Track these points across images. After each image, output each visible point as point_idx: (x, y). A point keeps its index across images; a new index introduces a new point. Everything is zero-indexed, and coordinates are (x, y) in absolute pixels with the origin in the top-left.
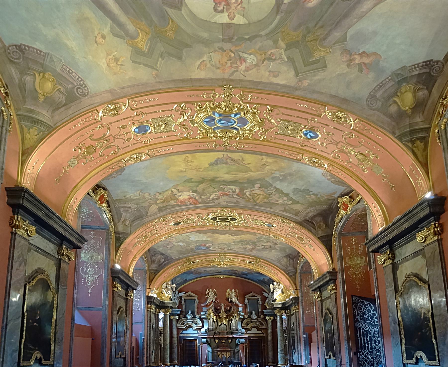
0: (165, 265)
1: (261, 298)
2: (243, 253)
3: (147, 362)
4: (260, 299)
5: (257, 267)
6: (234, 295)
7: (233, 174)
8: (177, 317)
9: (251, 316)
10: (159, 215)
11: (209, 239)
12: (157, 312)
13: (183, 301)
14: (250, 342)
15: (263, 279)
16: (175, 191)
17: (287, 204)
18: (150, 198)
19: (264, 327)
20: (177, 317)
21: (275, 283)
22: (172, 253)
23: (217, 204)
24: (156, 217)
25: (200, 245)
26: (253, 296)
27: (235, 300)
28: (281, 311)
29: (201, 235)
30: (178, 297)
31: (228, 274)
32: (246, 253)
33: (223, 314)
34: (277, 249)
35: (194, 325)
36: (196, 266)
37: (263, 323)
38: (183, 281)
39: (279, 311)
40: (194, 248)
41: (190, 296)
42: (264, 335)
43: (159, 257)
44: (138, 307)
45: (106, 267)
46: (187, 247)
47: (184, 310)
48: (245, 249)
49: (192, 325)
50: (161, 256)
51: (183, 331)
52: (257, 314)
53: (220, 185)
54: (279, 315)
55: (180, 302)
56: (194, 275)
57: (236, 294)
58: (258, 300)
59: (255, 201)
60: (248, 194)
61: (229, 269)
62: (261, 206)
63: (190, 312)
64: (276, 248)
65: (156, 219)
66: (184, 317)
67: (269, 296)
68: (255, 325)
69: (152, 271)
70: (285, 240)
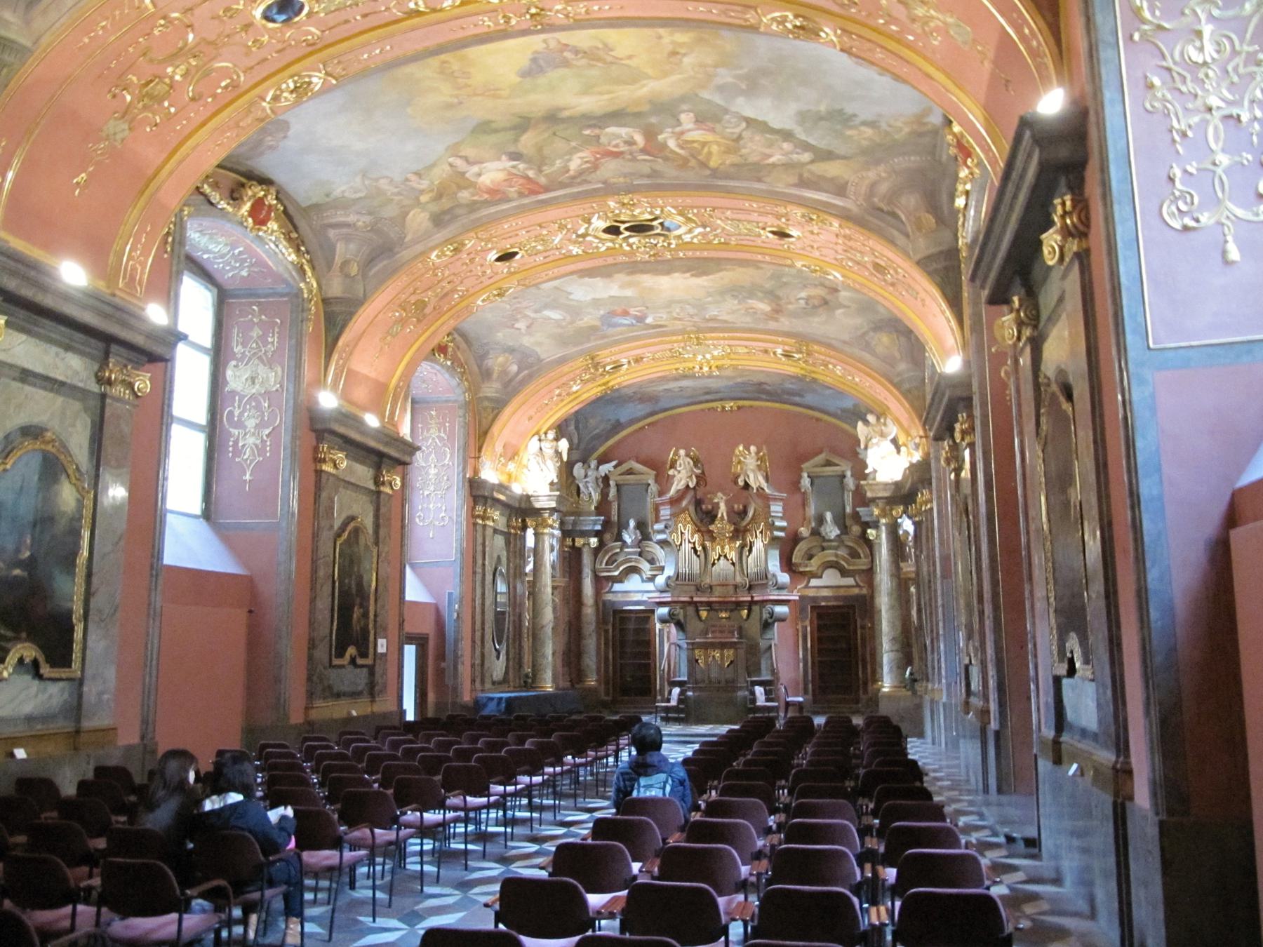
0: (524, 382)
2: (752, 325)
3: (473, 681)
4: (849, 473)
5: (809, 368)
6: (751, 462)
7: (601, 93)
8: (594, 541)
9: (822, 529)
10: (440, 236)
11: (628, 293)
12: (514, 528)
13: (613, 492)
14: (820, 616)
16: (459, 163)
17: (803, 165)
18: (396, 190)
19: (862, 564)
20: (594, 541)
21: (871, 418)
22: (540, 344)
23: (600, 185)
24: (431, 244)
25: (613, 314)
26: (828, 463)
27: (757, 480)
28: (891, 510)
29: (598, 282)
30: (597, 479)
31: (744, 395)
32: (761, 326)
33: (722, 525)
34: (849, 307)
35: (645, 566)
36: (626, 377)
38: (609, 427)
39: (883, 510)
40: (598, 323)
41: (630, 472)
42: (864, 591)
43: (501, 359)
44: (443, 514)
45: (291, 402)
46: (572, 322)
47: (615, 518)
48: (752, 312)
49: (640, 566)
50: (507, 355)
51: (613, 582)
52: (841, 521)
53: (581, 129)
54: (885, 525)
55: (604, 495)
56: (640, 407)
57: (759, 459)
58: (844, 476)
59: (704, 165)
60: (672, 144)
61: (739, 380)
62: (728, 177)
63: (632, 523)
64: (846, 303)
65: (432, 249)
66: (615, 541)
68: (834, 559)
69: (486, 404)
70: (843, 276)
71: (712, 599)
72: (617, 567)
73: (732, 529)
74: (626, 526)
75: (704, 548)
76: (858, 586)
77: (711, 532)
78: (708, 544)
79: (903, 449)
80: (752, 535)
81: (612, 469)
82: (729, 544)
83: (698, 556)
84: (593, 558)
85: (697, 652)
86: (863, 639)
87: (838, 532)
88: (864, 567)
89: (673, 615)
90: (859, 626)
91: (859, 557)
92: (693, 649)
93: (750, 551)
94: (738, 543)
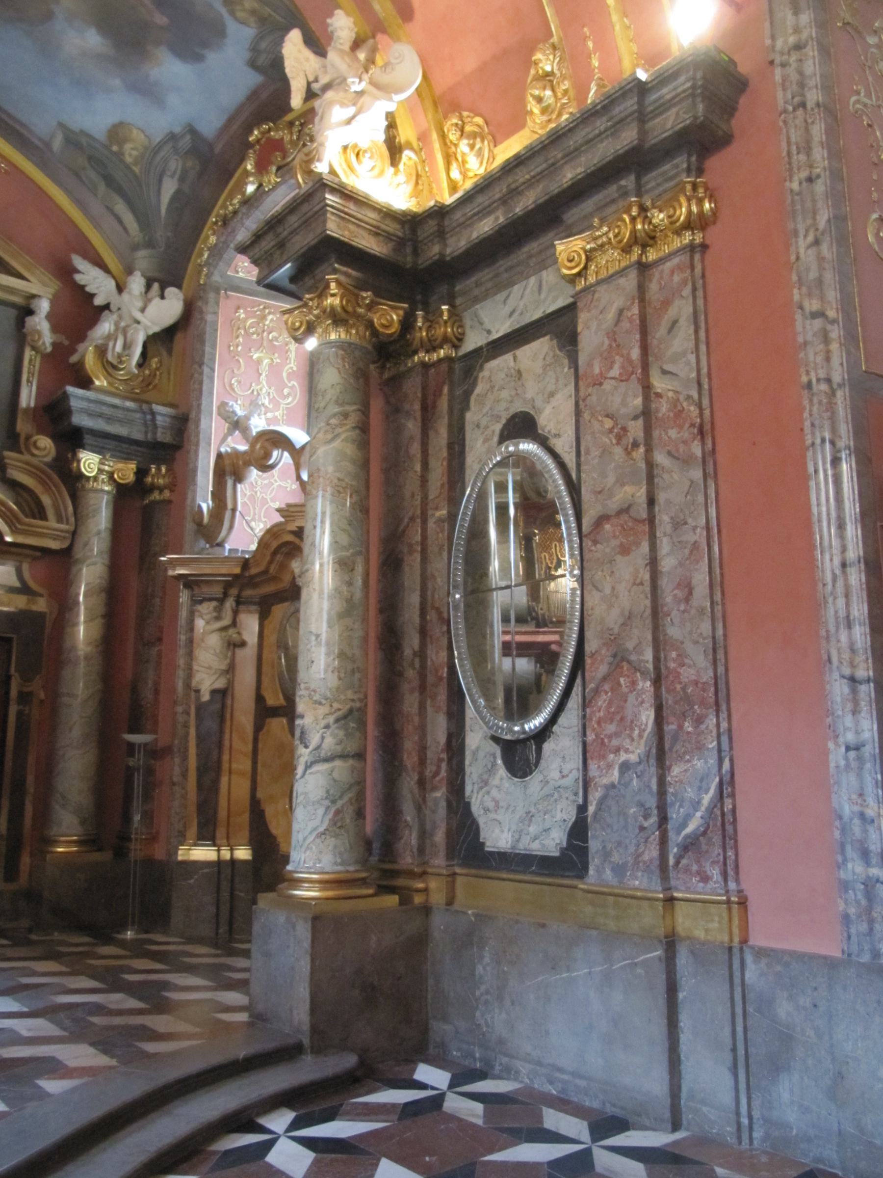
1: (53, 302)
4: (44, 306)
15: (117, 132)
37: (46, 500)
42: (41, 605)
76: (24, 589)
79: (407, 155)
88: (54, 545)
90: (14, 693)
91: (43, 516)
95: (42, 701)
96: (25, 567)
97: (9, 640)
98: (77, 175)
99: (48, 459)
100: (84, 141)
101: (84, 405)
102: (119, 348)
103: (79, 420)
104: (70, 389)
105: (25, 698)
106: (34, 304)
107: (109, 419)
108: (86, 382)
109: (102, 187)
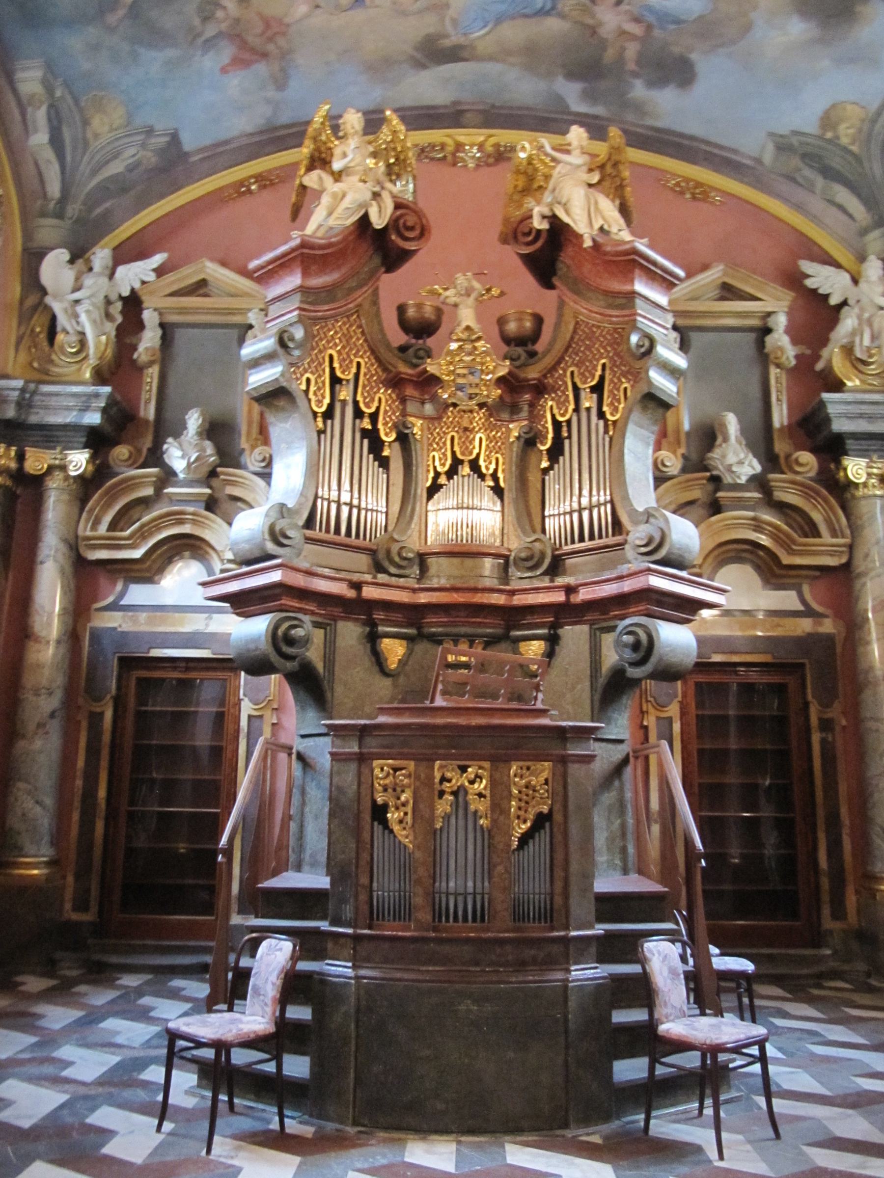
1: (790, 314)
9: (716, 454)
26: (728, 292)
30: (108, 302)
37: (817, 517)
38: (150, 158)
42: (828, 627)
47: (149, 412)
63: (194, 421)
67: (852, 294)
71: (423, 598)
72: (143, 534)
73: (502, 372)
74: (178, 431)
75: (404, 439)
77: (430, 382)
78: (417, 427)
80: (562, 404)
81: (151, 277)
82: (488, 428)
83: (384, 463)
84: (76, 510)
85: (380, 769)
86: (829, 757)
87: (758, 468)
89: (290, 641)
91: (816, 534)
92: (363, 759)
93: (555, 453)
94: (515, 429)
95: (844, 727)
96: (806, 589)
97: (802, 665)
98: (793, 180)
99: (812, 474)
100: (795, 141)
101: (842, 409)
102: (867, 342)
103: (839, 426)
104: (826, 396)
105: (826, 725)
106: (771, 322)
107: (871, 418)
108: (837, 386)
109: (820, 182)
